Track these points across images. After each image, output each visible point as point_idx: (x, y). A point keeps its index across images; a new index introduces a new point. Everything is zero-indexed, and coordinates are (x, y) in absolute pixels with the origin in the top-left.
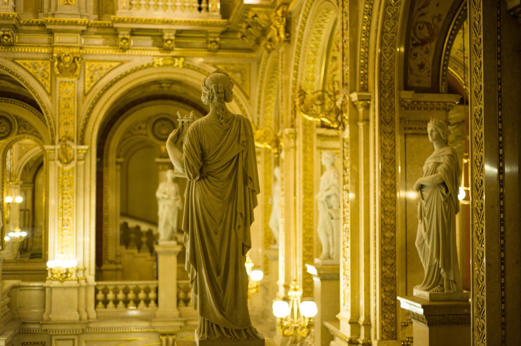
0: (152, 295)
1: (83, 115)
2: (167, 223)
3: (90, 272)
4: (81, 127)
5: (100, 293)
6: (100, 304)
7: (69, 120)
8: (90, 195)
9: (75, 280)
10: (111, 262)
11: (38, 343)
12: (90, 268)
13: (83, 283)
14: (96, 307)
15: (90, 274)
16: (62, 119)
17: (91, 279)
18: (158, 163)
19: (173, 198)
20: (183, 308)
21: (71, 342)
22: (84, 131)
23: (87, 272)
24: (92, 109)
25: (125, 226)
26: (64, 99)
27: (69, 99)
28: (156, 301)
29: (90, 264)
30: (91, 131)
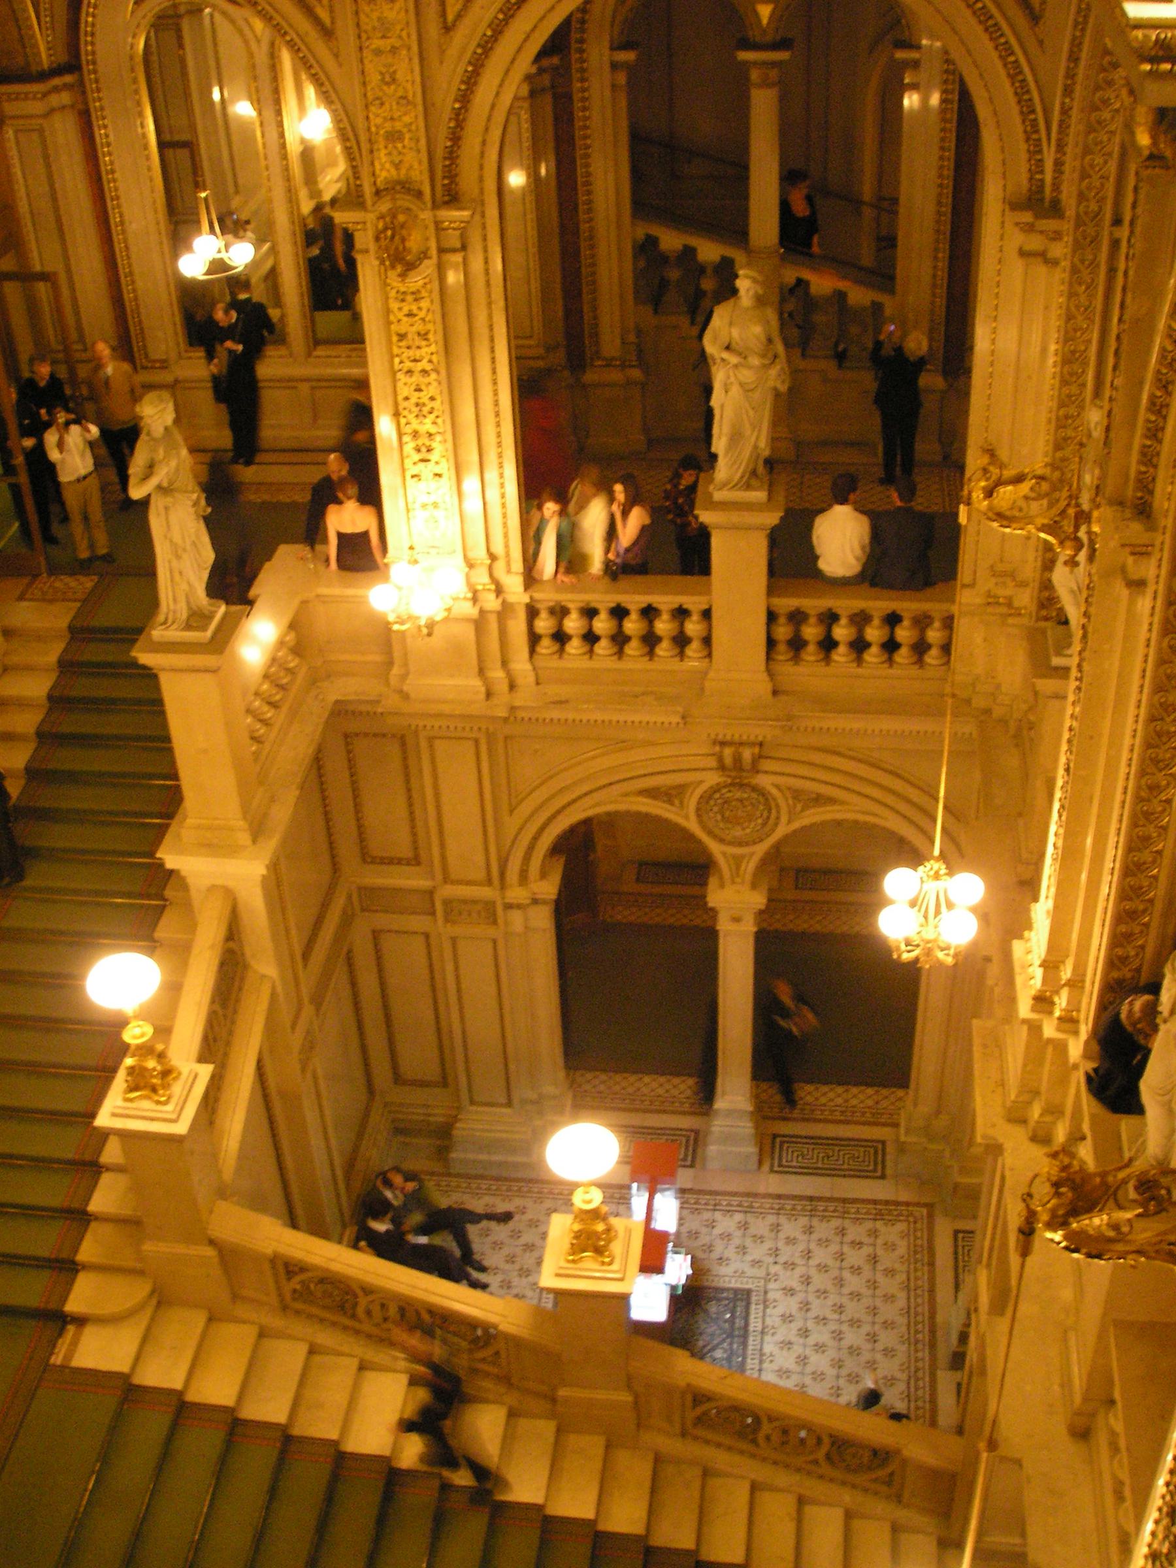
0: (693, 627)
1: (446, 102)
2: (736, 438)
3: (508, 564)
4: (442, 142)
5: (544, 615)
6: (546, 646)
7: (398, 125)
8: (492, 350)
9: (465, 599)
10: (609, 364)
11: (384, 735)
12: (508, 555)
13: (491, 602)
14: (532, 651)
15: (509, 571)
16: (379, 121)
17: (514, 584)
18: (746, 64)
19: (755, 361)
20: (787, 670)
21: (469, 746)
22: (452, 156)
23: (500, 566)
24: (471, 81)
25: (647, 247)
26: (378, 52)
27: (394, 50)
28: (707, 641)
29: (507, 546)
30: (477, 150)
